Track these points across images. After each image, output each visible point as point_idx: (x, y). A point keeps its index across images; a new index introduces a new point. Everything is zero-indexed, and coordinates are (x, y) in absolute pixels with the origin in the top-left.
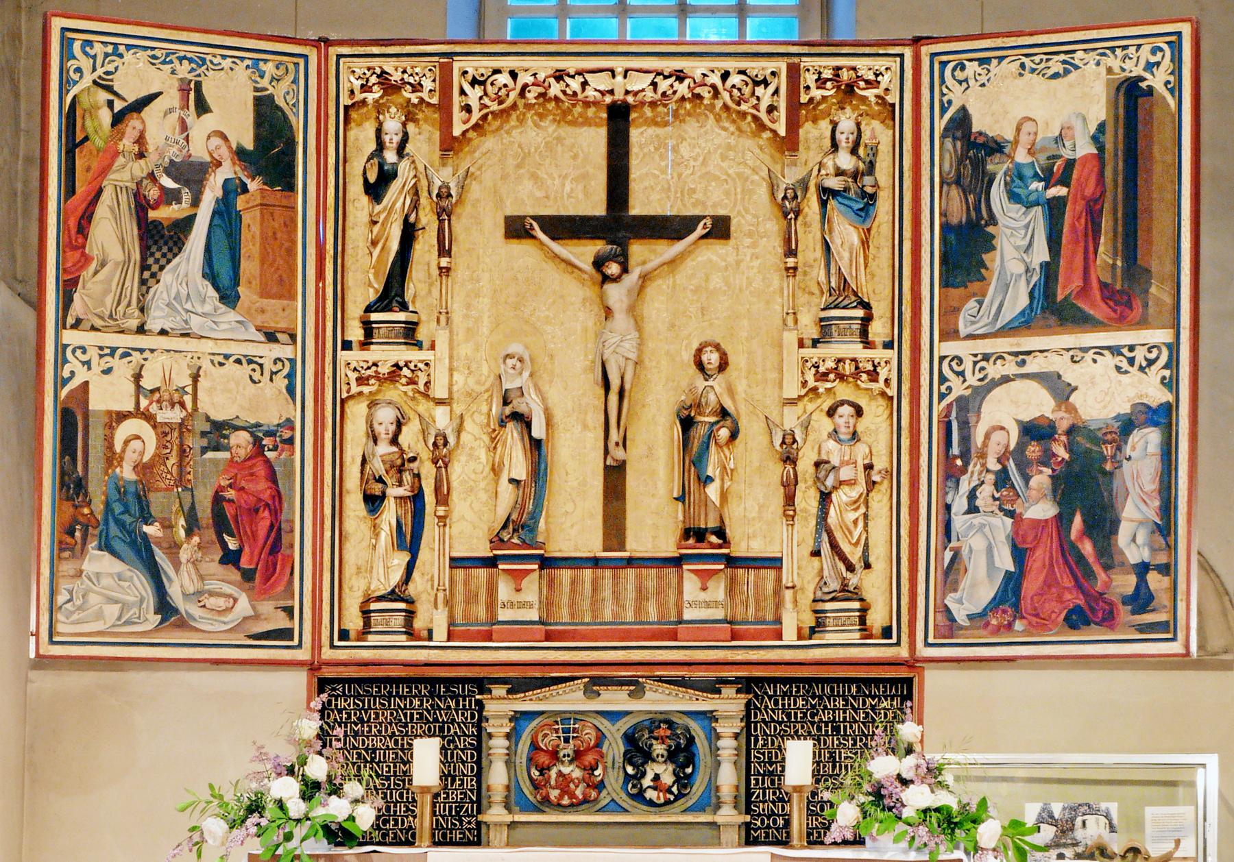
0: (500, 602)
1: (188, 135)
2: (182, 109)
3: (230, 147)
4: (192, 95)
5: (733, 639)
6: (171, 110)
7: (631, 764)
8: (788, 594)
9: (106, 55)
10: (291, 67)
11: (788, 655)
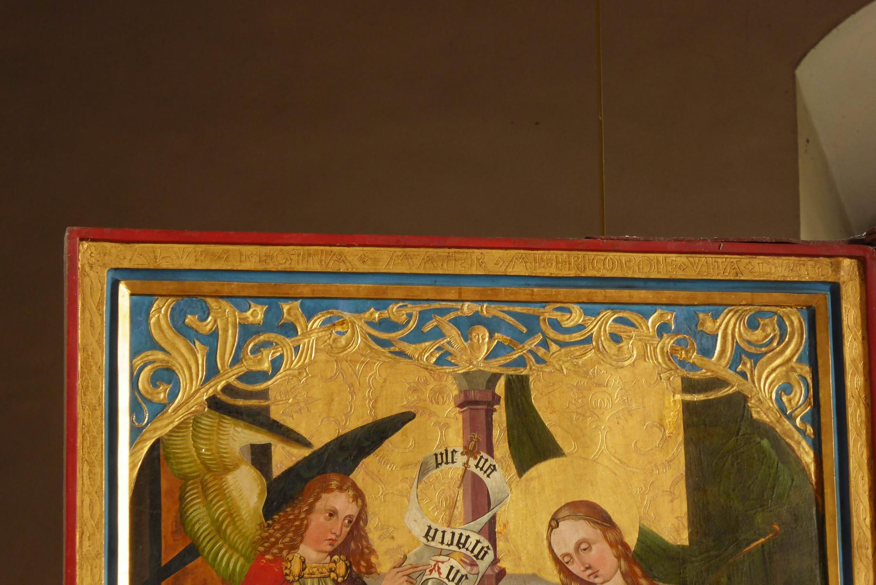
1: (492, 521)
2: (469, 452)
3: (618, 544)
4: (500, 416)
6: (442, 458)
9: (247, 331)
10: (796, 320)
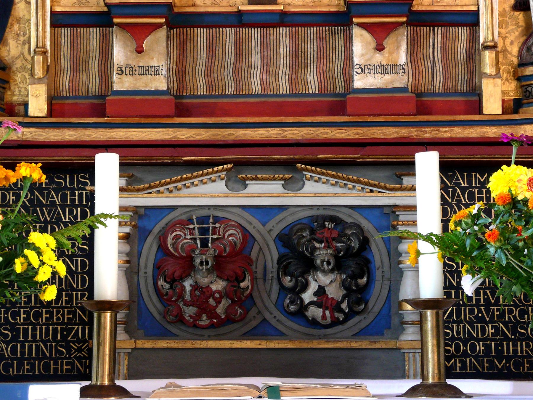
0: (116, 67)
5: (419, 112)
7: (286, 274)
8: (488, 56)
11: (491, 132)
